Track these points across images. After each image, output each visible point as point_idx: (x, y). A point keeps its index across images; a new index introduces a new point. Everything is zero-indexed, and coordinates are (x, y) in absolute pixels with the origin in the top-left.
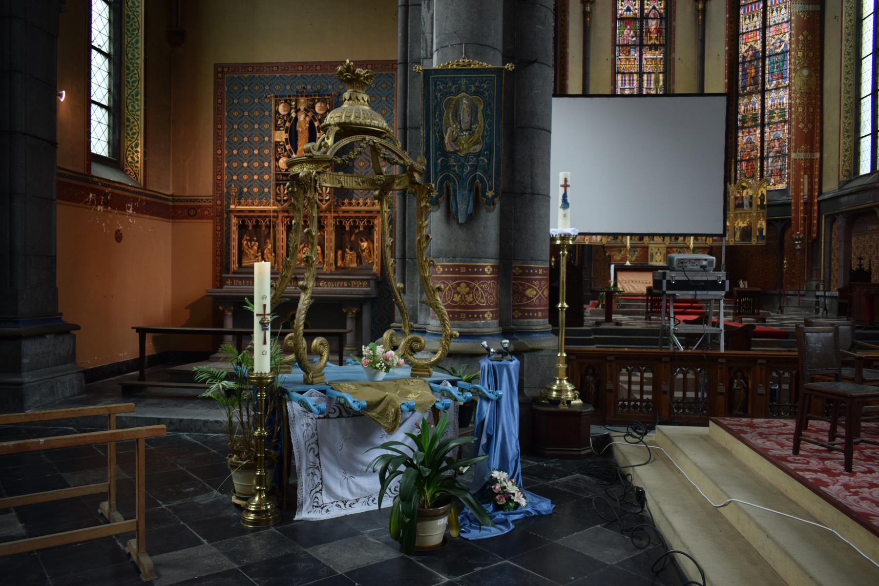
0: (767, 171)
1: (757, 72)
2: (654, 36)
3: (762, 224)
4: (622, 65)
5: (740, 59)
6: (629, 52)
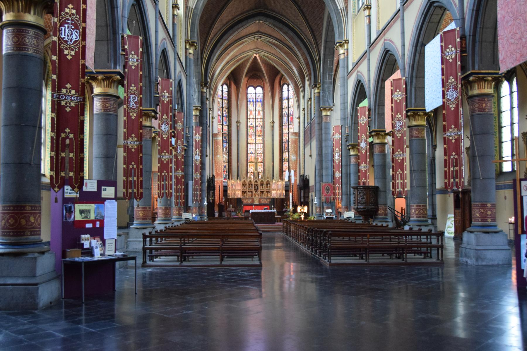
3: (284, 192)
4: (249, 141)
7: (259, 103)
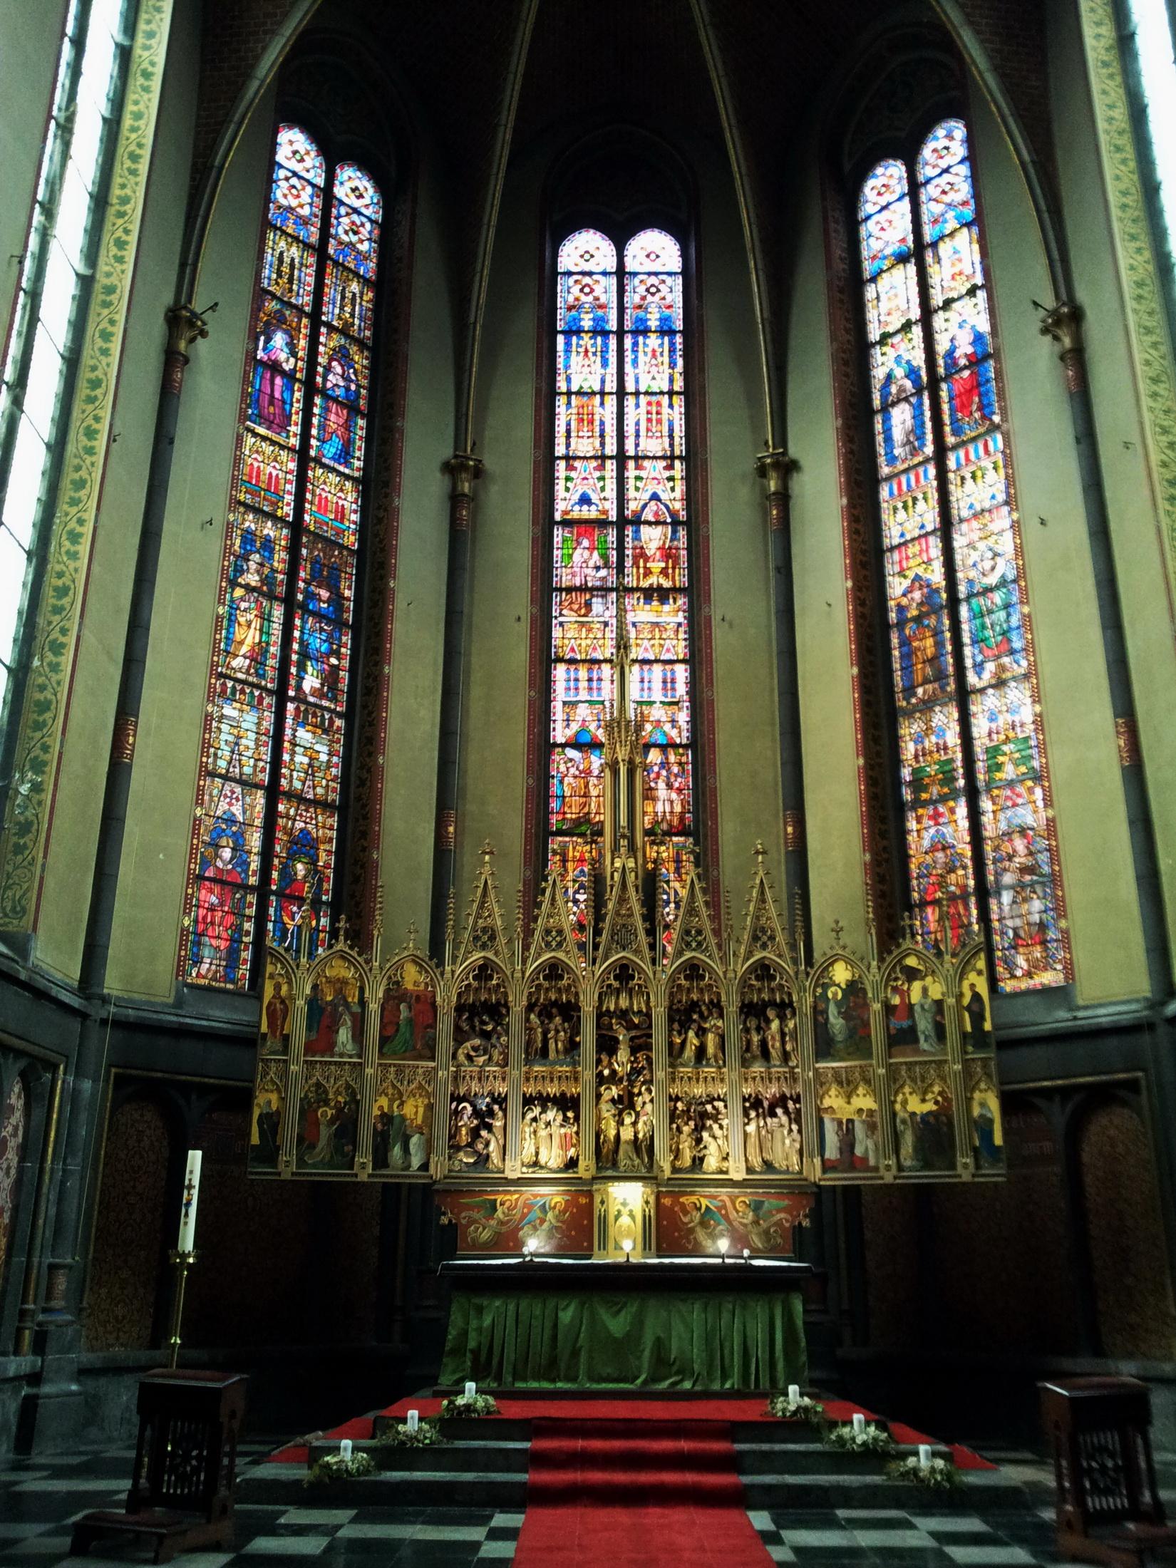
0: (1003, 933)
1: (939, 645)
2: (657, 566)
3: (988, 1102)
5: (893, 616)
6: (588, 605)
7: (653, 341)
